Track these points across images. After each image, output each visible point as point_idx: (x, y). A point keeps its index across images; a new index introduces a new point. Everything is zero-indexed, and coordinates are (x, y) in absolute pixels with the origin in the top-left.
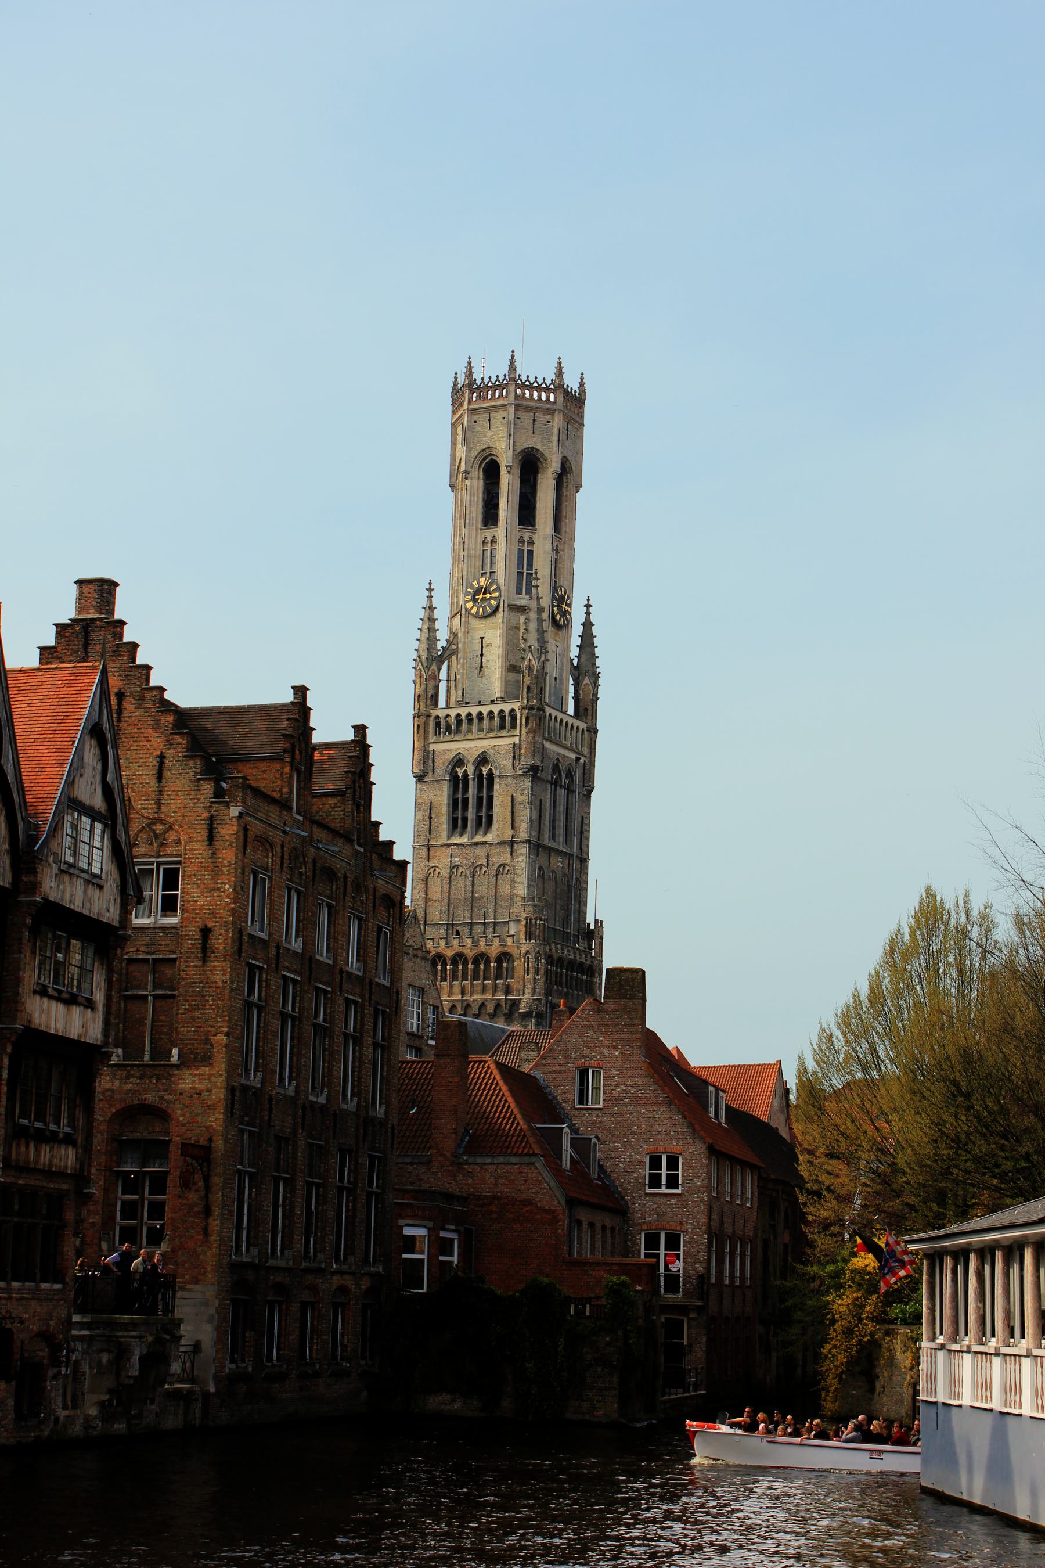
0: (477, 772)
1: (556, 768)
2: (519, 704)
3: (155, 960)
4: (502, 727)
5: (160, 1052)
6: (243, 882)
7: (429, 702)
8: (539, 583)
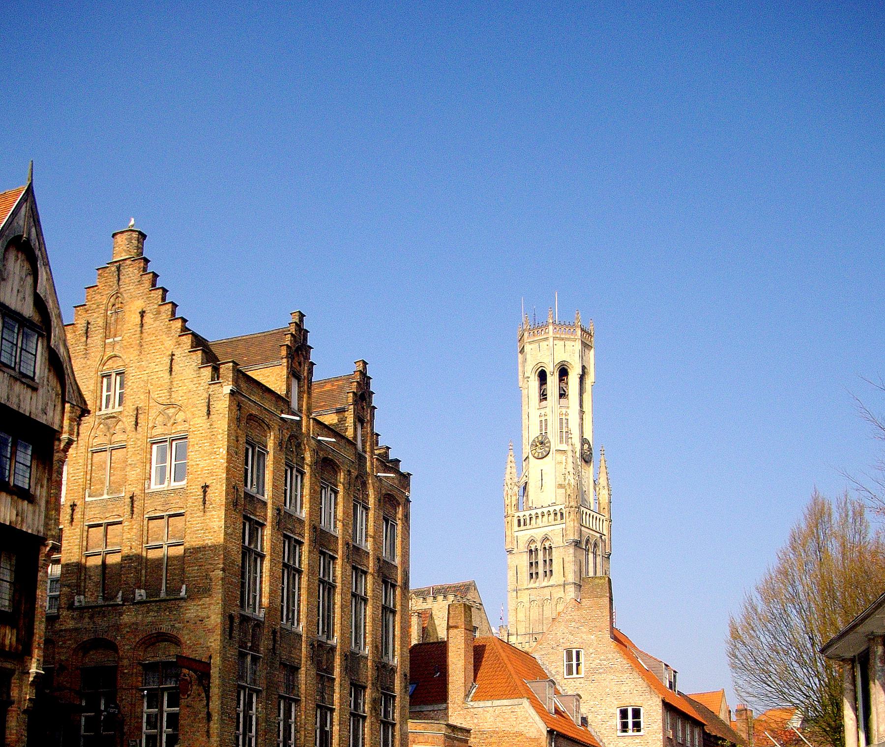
0: (543, 547)
1: (587, 541)
2: (564, 505)
3: (170, 516)
4: (555, 520)
5: (173, 591)
6: (237, 448)
7: (513, 509)
8: (572, 436)
